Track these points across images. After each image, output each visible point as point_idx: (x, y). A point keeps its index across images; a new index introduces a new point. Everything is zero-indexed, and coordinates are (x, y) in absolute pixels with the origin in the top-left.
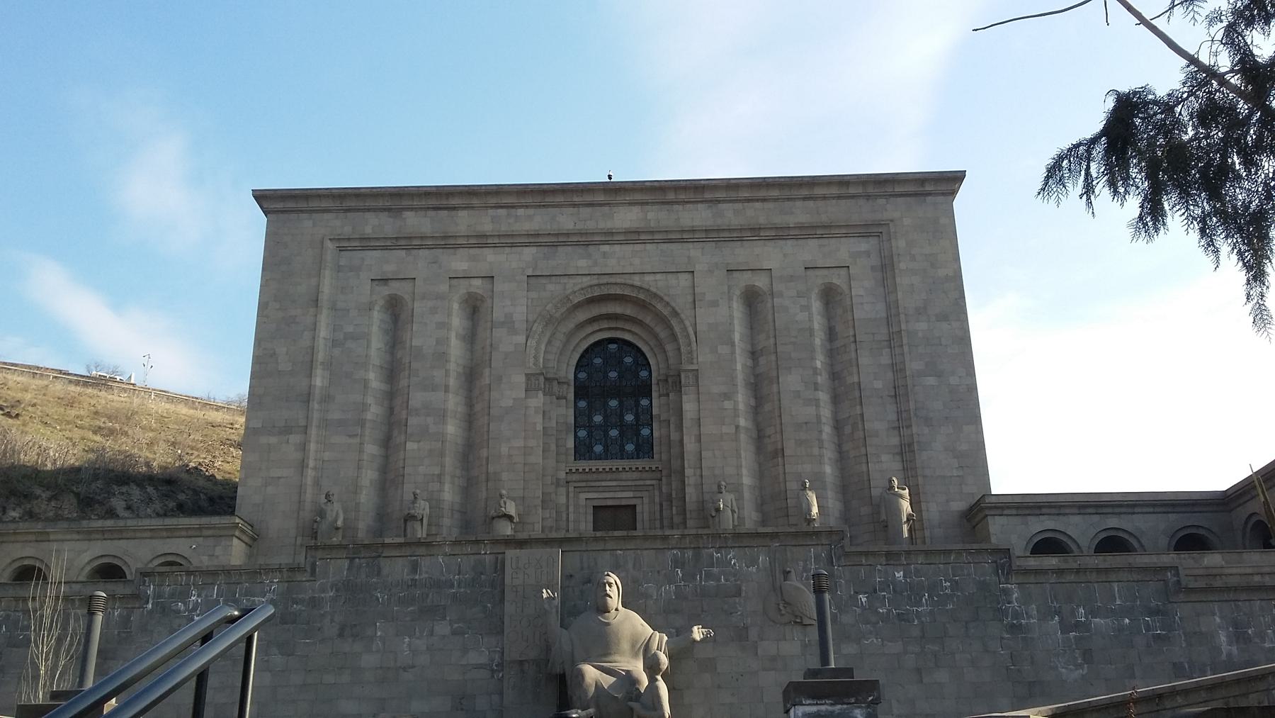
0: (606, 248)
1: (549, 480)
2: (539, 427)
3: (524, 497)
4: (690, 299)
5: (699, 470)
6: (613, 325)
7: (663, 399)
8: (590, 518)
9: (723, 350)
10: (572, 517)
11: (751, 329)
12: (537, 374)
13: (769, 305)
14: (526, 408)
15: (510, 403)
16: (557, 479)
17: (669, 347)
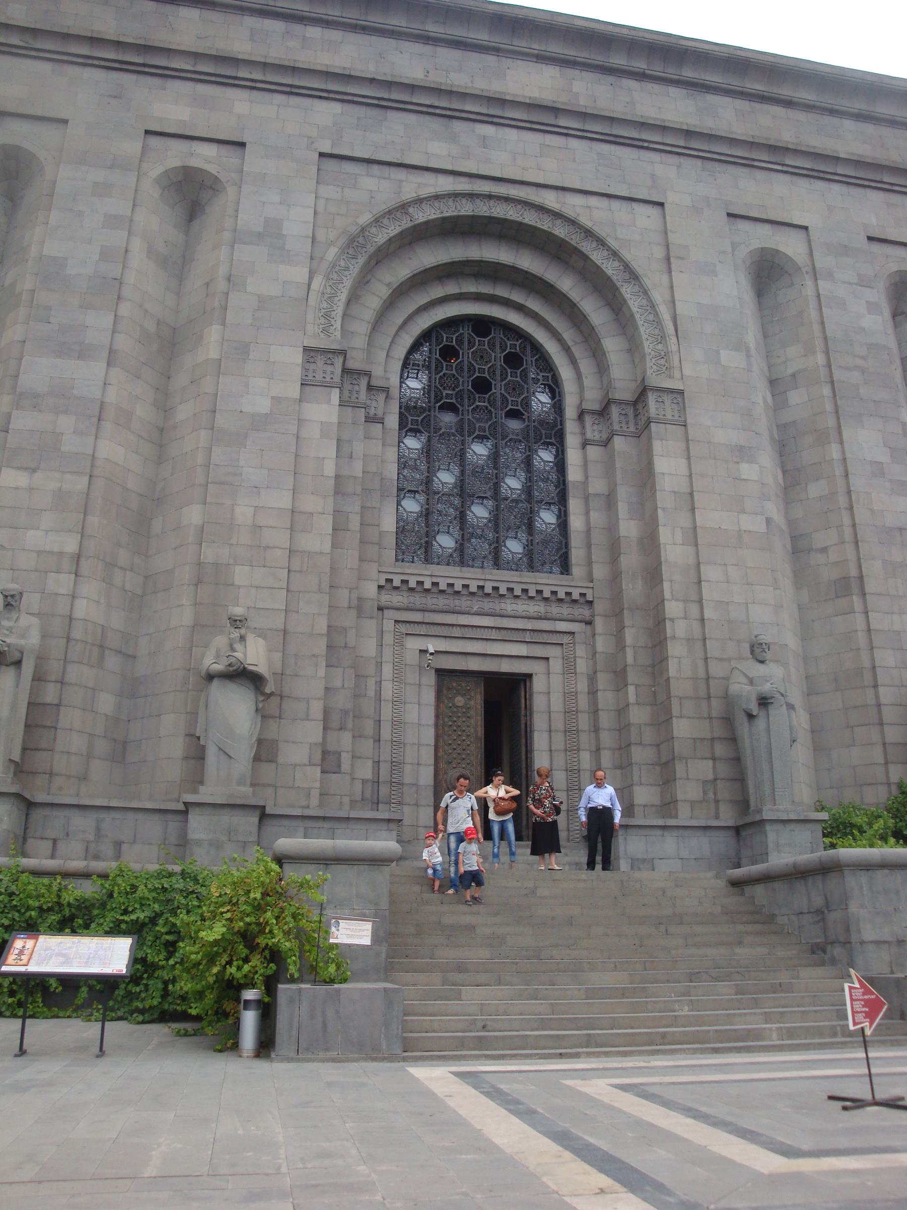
0: (489, 130)
1: (343, 596)
2: (330, 469)
3: (285, 632)
4: (659, 253)
5: (694, 610)
6: (486, 288)
7: (593, 452)
8: (429, 696)
9: (730, 359)
10: (388, 690)
11: (765, 336)
12: (335, 352)
13: (809, 291)
14: (300, 422)
15: (263, 405)
16: (360, 599)
17: (612, 345)
